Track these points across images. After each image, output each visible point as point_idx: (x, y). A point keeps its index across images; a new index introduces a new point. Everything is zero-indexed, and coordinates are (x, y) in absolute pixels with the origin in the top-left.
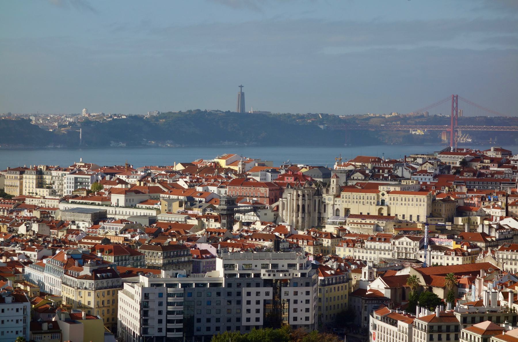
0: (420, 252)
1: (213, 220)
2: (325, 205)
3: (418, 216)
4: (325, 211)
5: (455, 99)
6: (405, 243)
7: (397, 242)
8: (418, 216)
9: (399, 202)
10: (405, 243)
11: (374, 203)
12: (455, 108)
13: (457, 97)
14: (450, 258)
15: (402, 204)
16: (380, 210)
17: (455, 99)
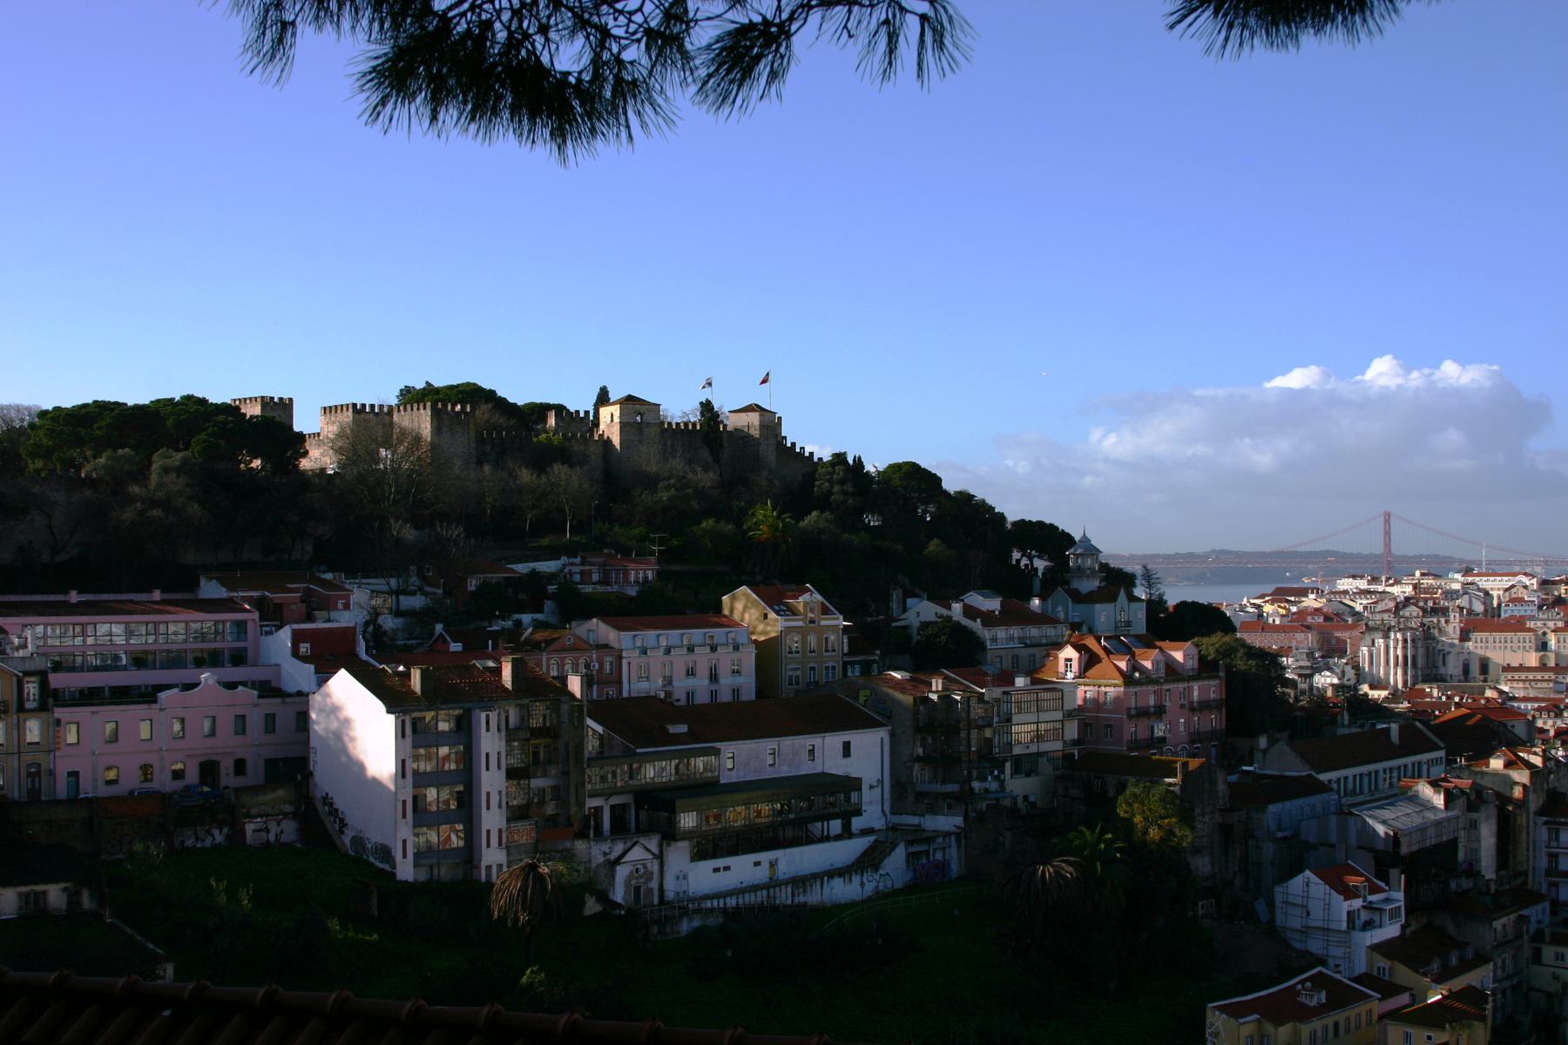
16: (1541, 658)
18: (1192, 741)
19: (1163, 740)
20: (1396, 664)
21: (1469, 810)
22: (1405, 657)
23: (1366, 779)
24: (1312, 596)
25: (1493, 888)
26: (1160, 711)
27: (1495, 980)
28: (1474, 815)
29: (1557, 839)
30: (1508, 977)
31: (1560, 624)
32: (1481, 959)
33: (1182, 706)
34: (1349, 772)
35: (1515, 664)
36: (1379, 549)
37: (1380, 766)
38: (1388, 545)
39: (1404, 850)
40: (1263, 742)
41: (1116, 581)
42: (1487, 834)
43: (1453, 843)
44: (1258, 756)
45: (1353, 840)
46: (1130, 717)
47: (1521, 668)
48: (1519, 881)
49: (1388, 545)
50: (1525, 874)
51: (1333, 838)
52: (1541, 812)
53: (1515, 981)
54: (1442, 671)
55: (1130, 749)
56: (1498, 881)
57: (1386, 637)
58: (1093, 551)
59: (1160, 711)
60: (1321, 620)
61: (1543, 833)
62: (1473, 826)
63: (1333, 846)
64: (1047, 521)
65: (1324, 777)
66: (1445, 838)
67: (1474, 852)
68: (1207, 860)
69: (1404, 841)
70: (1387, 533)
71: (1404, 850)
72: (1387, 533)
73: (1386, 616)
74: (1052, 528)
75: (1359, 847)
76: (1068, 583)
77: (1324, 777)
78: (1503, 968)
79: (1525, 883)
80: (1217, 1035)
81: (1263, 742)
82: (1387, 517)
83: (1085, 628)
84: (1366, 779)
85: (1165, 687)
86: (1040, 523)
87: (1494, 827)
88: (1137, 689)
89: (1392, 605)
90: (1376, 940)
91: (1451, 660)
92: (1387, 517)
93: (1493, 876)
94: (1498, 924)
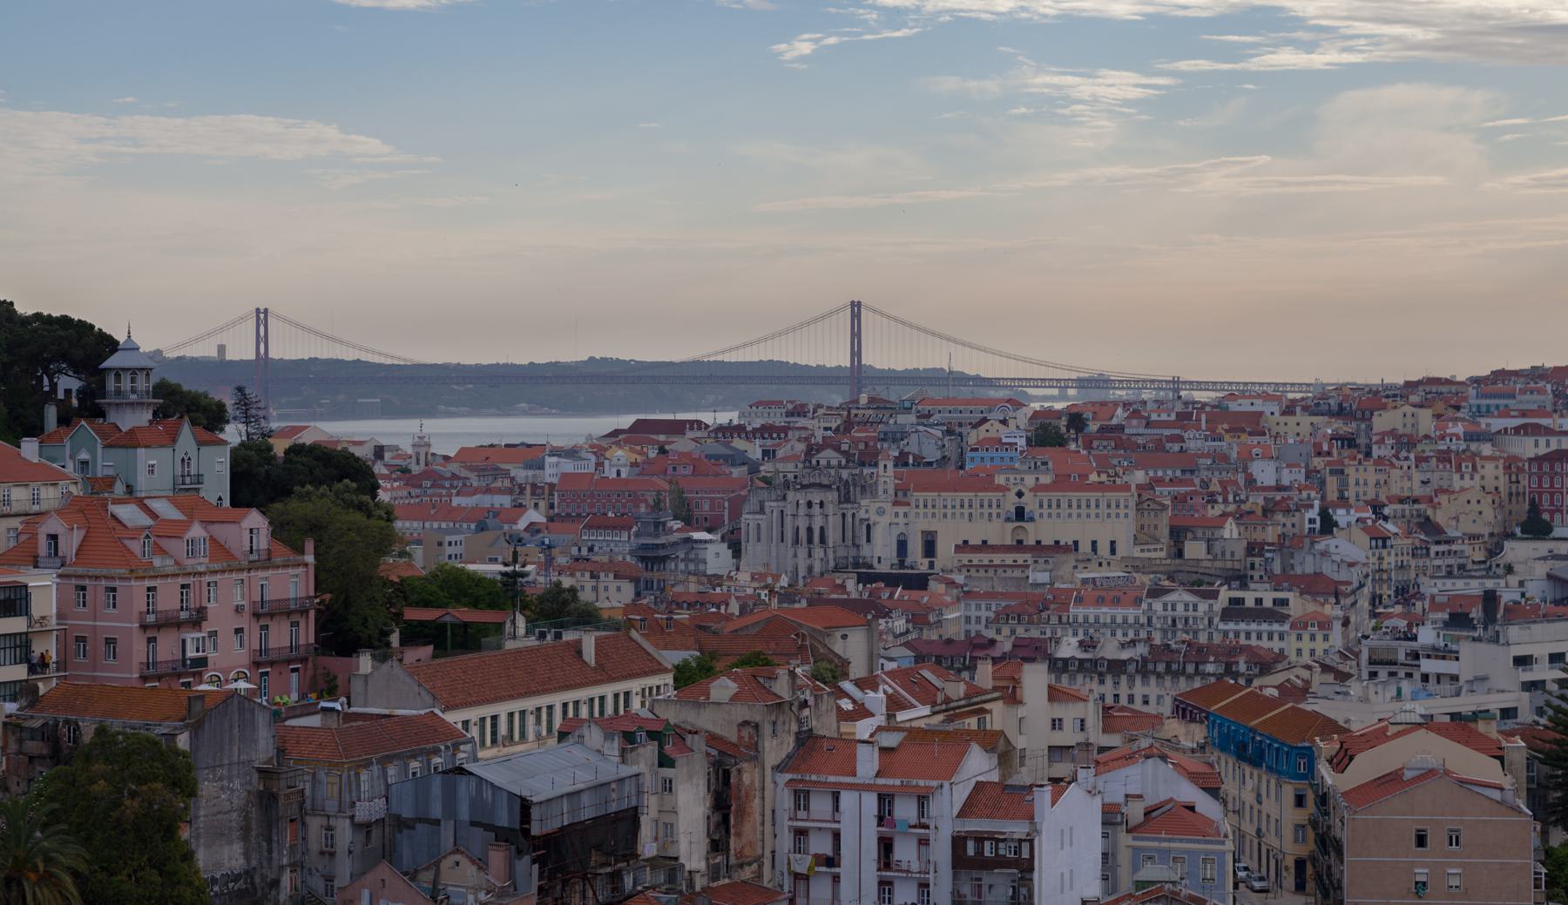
0: (1222, 626)
1: (611, 576)
2: (868, 527)
3: (1113, 543)
4: (868, 540)
5: (262, 317)
6: (1180, 608)
7: (1157, 606)
8: (1113, 543)
9: (1064, 510)
10: (1180, 608)
11: (998, 515)
12: (262, 339)
13: (266, 311)
14: (1306, 637)
15: (1070, 515)
17: (262, 317)
18: (257, 664)
19: (202, 662)
20: (796, 541)
21: (661, 765)
22: (810, 530)
23: (531, 720)
24: (690, 434)
25: (699, 883)
28: (667, 772)
29: (807, 808)
31: (1046, 479)
33: (238, 610)
34: (502, 709)
35: (975, 541)
36: (836, 356)
37: (530, 704)
38: (856, 353)
39: (536, 830)
40: (365, 663)
42: (691, 803)
43: (631, 818)
44: (357, 686)
45: (464, 813)
47: (985, 546)
48: (747, 873)
49: (856, 353)
50: (759, 860)
51: (436, 811)
52: (778, 768)
54: (865, 551)
55: (144, 679)
56: (714, 873)
57: (784, 498)
60: (689, 471)
61: (786, 800)
62: (668, 786)
63: (437, 822)
65: (454, 718)
66: (613, 807)
67: (667, 831)
68: (237, 848)
69: (535, 813)
70: (856, 335)
71: (536, 830)
72: (856, 335)
73: (790, 467)
74: (84, 328)
75: (473, 824)
76: (103, 415)
77: (454, 718)
79: (759, 875)
81: (365, 663)
82: (856, 308)
83: (119, 489)
84: (531, 720)
85: (208, 578)
86: (65, 321)
87: (703, 789)
89: (801, 447)
91: (878, 533)
92: (856, 308)
93: (702, 866)
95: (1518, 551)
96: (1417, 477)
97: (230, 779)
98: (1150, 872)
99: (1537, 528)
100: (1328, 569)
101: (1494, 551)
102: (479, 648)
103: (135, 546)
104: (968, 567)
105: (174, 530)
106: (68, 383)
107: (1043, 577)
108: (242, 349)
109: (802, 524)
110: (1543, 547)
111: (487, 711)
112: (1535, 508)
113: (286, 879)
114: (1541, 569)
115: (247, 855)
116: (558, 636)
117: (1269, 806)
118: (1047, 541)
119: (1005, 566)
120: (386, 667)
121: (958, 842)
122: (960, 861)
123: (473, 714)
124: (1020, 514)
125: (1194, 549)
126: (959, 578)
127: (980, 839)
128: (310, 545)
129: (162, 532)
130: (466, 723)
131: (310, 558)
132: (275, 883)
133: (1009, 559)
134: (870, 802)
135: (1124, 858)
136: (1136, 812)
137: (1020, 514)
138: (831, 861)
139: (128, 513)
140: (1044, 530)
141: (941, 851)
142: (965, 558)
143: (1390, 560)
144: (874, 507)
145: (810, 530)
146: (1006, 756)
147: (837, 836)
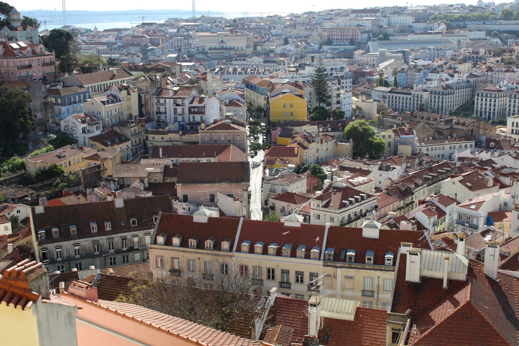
26: (30, 66)
27: (132, 146)
30: (138, 145)
32: (127, 140)
35: (213, 47)
36: (190, 9)
38: (194, 7)
41: (29, 23)
46: (18, 68)
47: (215, 49)
49: (194, 7)
53: (140, 146)
58: (18, 13)
59: (30, 66)
64: (4, 2)
70: (193, 3)
72: (193, 3)
74: (6, 5)
78: (135, 142)
79: (150, 117)
80: (29, 167)
83: (14, 39)
85: (32, 58)
88: (21, 60)
90: (92, 136)
94: (132, 129)
95: (325, 48)
96: (305, 32)
97: (37, 100)
98: (228, 114)
99: (329, 42)
100: (286, 52)
101: (321, 47)
102: (91, 72)
103: (15, 52)
104: (212, 53)
105: (25, 48)
106: (3, 17)
107: (227, 55)
108: (60, 9)
109: (176, 44)
110: (330, 47)
111: (93, 85)
112: (329, 39)
113: (50, 120)
114: (329, 51)
115: (42, 115)
116: (109, 69)
117: (259, 100)
118: (228, 47)
119: (219, 53)
120: (71, 76)
121: (190, 108)
122: (190, 112)
123: (90, 85)
124: (222, 42)
125: (259, 48)
126: (210, 56)
127: (194, 107)
128: (54, 51)
129: (22, 48)
130: (88, 87)
131: (54, 54)
132: (48, 121)
133: (220, 51)
134: (172, 101)
135: (225, 110)
136: (227, 101)
137: (222, 42)
138: (166, 113)
139: (14, 46)
140: (228, 45)
141: (187, 111)
142: (211, 51)
143: (299, 50)
144: (192, 40)
145: (178, 46)
146: (201, 92)
147: (166, 108)
